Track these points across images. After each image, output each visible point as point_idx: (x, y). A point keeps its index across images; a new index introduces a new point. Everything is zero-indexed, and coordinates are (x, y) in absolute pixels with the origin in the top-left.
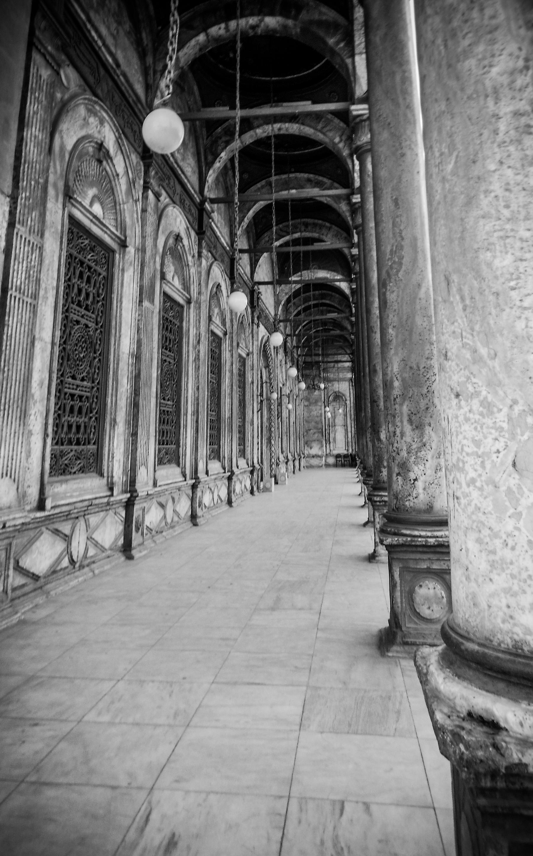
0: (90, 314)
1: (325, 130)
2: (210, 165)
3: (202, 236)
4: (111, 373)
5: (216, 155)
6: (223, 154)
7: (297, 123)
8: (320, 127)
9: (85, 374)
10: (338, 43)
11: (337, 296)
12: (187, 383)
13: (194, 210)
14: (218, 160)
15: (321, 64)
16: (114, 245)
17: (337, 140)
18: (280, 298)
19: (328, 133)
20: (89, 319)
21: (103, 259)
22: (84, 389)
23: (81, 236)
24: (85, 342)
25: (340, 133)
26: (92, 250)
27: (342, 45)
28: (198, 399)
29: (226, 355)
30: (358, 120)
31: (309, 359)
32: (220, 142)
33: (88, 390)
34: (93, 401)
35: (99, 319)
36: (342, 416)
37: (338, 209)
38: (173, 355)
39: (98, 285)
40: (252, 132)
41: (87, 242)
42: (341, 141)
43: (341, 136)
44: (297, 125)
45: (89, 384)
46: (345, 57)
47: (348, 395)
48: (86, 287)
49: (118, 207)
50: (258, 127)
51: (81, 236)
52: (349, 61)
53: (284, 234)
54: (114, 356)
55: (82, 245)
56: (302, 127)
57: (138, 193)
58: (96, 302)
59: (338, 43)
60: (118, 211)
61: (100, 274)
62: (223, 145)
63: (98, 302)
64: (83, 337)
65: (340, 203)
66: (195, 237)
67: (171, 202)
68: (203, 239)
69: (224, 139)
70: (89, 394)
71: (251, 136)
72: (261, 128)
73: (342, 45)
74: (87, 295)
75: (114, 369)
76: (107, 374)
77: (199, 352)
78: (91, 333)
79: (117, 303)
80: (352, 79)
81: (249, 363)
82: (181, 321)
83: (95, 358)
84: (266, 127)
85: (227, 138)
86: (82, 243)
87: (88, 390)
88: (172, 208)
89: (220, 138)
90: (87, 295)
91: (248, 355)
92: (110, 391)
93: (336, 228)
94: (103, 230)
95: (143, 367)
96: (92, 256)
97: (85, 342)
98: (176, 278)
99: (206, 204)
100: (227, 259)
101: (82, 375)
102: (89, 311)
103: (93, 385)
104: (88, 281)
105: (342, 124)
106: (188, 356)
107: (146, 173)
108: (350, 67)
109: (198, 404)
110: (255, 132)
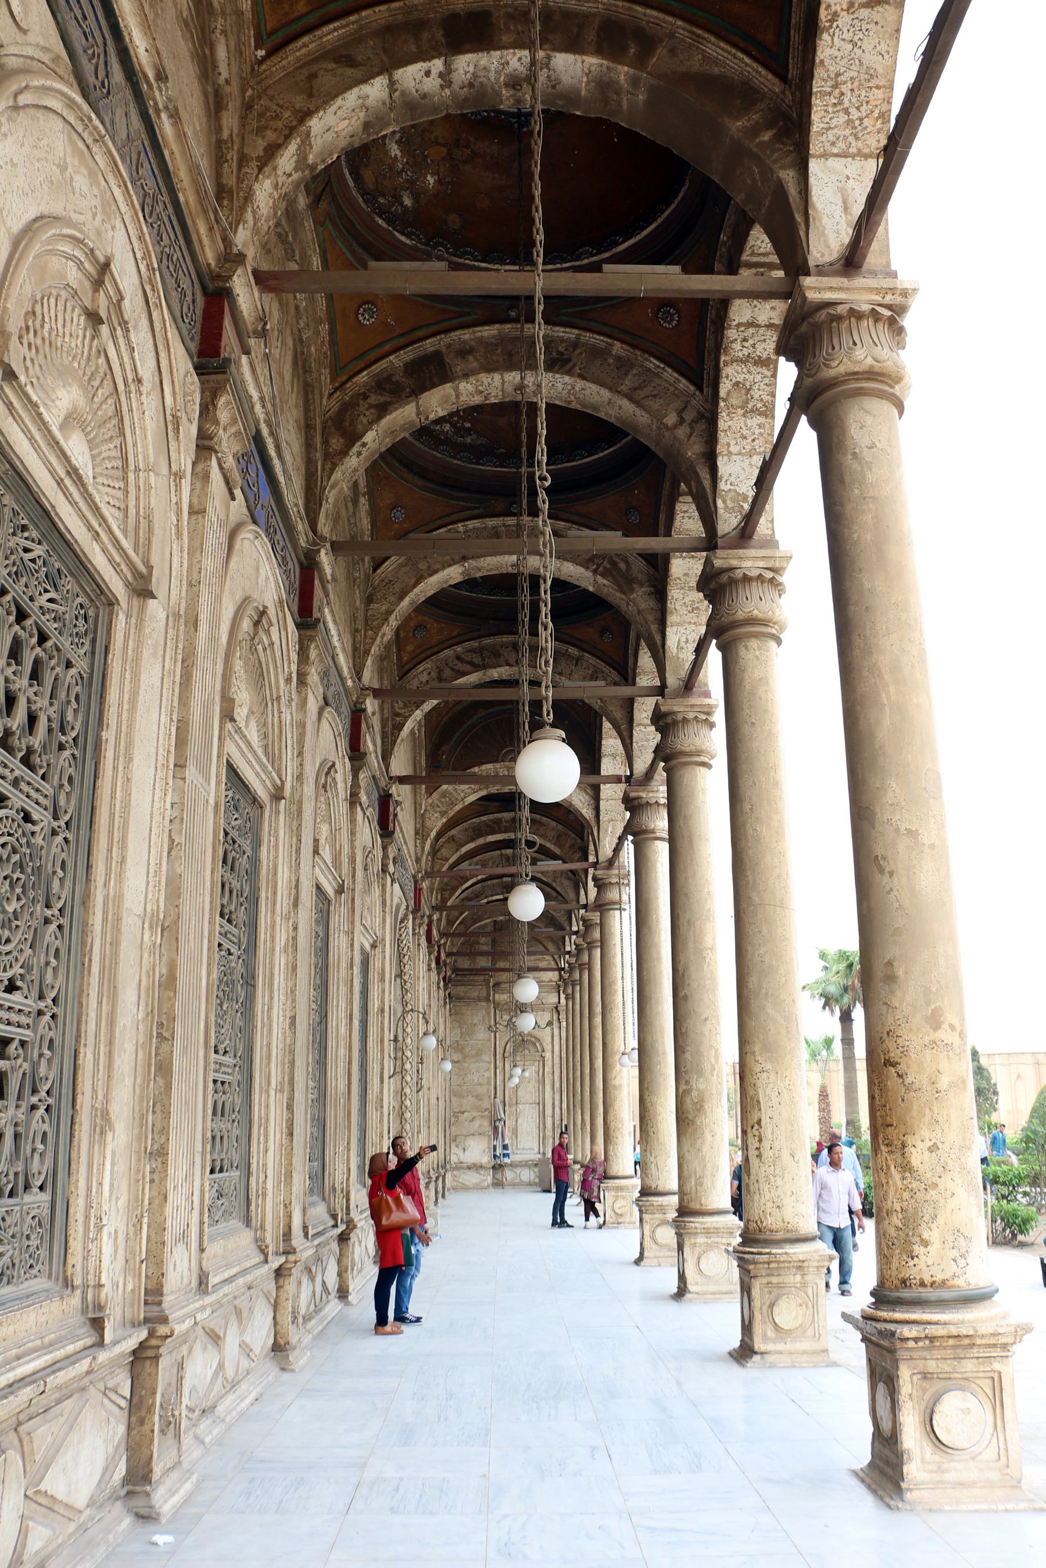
0: (35, 779)
1: (640, 394)
2: (333, 459)
3: (309, 633)
4: (95, 969)
5: (352, 437)
6: (369, 437)
7: (569, 373)
8: (628, 383)
9: (17, 970)
10: (754, 131)
11: (553, 824)
12: (270, 1009)
13: (294, 566)
14: (355, 449)
15: (676, 201)
16: (117, 587)
17: (671, 419)
18: (428, 823)
19: (646, 402)
20: (33, 793)
21: (81, 621)
22: (14, 1017)
23: (24, 528)
24: (21, 866)
25: (678, 404)
26: (53, 580)
27: (766, 136)
28: (292, 1052)
29: (339, 943)
30: (822, 315)
31: (464, 963)
32: (363, 405)
33: (24, 1020)
34: (41, 1055)
35: (62, 801)
36: (533, 1082)
37: (623, 606)
38: (235, 931)
39: (63, 696)
40: (448, 388)
41: (38, 551)
42: (682, 421)
43: (680, 413)
44: (567, 378)
45: (32, 1004)
46: (775, 167)
47: (549, 1039)
48: (31, 692)
49: (131, 476)
50: (466, 376)
51: (24, 528)
52: (788, 177)
53: (469, 668)
54: (105, 920)
55: (27, 556)
56: (580, 384)
57: (185, 458)
58: (55, 746)
59: (754, 131)
60: (132, 488)
61: (69, 665)
62: (371, 413)
63: (61, 747)
64: (14, 851)
65: (632, 591)
66: (293, 632)
67: (249, 520)
68: (311, 639)
69: (374, 399)
70: (27, 1034)
71: (445, 400)
72: (472, 379)
73: (766, 136)
74: (32, 719)
75: (103, 959)
76: (84, 969)
77: (295, 929)
78: (38, 840)
79: (116, 758)
80: (799, 218)
81: (376, 965)
82: (257, 844)
83: (47, 921)
84: (485, 378)
85: (386, 398)
86: (26, 550)
87: (24, 1020)
88: (251, 536)
89: (365, 397)
90: (32, 719)
91: (374, 946)
92: (92, 1026)
93: (593, 660)
94: (90, 527)
95: (181, 961)
96: (50, 601)
97: (21, 866)
98: (253, 724)
99: (323, 552)
100: (346, 710)
101: (10, 974)
102: (32, 768)
103: (42, 1005)
104: (35, 675)
105: (684, 384)
106: (273, 937)
107: (207, 409)
108: (792, 190)
109: (292, 1063)
110: (456, 389)
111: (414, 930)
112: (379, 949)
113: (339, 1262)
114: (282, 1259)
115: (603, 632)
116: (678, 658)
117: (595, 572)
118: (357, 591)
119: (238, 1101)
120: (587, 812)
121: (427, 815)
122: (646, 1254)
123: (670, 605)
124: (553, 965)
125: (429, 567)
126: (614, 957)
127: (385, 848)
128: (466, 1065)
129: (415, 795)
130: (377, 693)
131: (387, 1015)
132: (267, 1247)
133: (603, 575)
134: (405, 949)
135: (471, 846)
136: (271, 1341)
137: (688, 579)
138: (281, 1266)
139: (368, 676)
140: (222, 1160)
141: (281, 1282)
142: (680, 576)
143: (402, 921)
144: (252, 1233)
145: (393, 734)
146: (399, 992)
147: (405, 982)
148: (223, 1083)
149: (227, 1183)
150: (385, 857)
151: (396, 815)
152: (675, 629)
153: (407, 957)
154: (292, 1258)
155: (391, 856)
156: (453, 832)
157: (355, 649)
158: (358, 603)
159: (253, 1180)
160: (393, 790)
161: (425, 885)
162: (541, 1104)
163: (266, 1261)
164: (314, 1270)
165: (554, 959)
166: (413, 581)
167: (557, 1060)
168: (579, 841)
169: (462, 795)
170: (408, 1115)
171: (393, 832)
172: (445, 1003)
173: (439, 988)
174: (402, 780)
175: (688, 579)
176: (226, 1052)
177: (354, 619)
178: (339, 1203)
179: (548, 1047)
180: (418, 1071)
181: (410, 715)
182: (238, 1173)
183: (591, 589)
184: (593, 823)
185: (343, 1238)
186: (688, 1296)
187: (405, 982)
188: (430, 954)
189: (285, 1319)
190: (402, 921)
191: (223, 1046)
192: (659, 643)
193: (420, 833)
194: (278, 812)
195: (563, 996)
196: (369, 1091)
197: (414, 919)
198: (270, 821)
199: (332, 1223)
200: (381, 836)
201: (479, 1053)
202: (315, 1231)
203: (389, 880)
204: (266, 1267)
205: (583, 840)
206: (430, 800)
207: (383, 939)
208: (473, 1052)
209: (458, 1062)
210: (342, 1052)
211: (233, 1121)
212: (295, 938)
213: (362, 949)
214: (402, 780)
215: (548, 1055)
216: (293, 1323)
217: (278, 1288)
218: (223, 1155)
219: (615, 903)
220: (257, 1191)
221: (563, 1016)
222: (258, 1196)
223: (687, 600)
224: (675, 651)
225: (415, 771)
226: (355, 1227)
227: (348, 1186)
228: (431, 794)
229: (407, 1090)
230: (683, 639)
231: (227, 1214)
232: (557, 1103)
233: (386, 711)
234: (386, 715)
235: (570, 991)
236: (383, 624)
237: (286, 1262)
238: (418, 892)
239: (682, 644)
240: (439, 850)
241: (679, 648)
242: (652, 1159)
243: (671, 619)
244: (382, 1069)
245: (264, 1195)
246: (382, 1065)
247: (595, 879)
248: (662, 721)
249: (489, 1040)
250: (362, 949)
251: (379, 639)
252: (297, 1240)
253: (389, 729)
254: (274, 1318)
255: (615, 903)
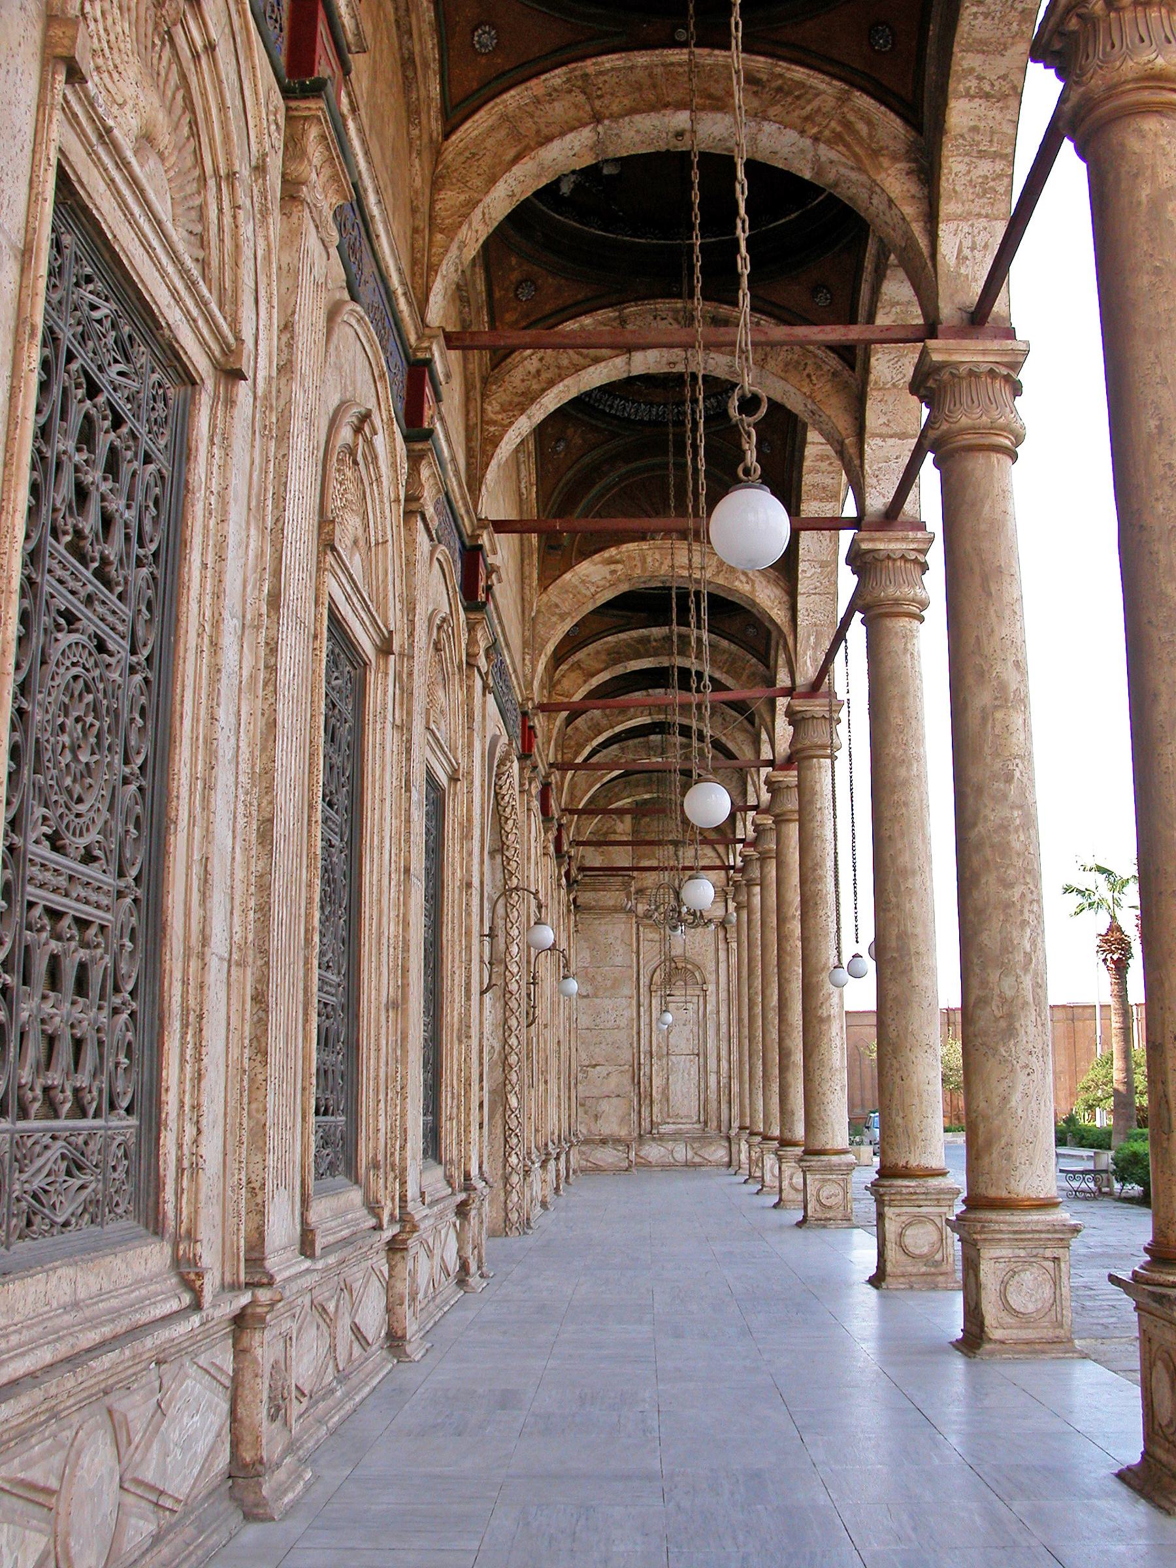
111: (521, 785)
112: (462, 786)
113: (388, 1288)
114: (245, 1299)
115: (815, 290)
116: (960, 274)
117: (816, 139)
118: (417, 162)
119: (130, 970)
120: (779, 615)
121: (541, 619)
122: (889, 1268)
123: (945, 185)
124: (718, 863)
125: (538, 132)
126: (822, 826)
127: (471, 628)
128: (597, 1001)
129: (523, 588)
130: (451, 341)
131: (475, 892)
132: (200, 1275)
133: (828, 142)
134: (508, 810)
135: (605, 676)
136: (223, 1460)
137: (978, 138)
138: (244, 1308)
139: (438, 310)
140: (77, 1091)
141: (245, 1342)
142: (965, 130)
143: (502, 763)
144: (168, 1249)
145: (483, 451)
146: (499, 876)
147: (509, 860)
148: (82, 924)
149: (94, 1146)
150: (472, 642)
151: (489, 589)
152: (953, 226)
153: (510, 822)
154: (264, 1295)
155: (483, 645)
156: (580, 655)
157: (414, 262)
158: (418, 183)
159: (168, 1140)
160: (485, 540)
161: (539, 722)
162: (700, 1054)
163: (197, 1306)
164: (331, 1307)
165: (719, 856)
166: (511, 154)
167: (723, 995)
168: (761, 668)
169: (593, 590)
170: (513, 1059)
171: (484, 604)
172: (569, 911)
173: (559, 885)
174: (500, 526)
175: (978, 138)
176: (88, 858)
177: (414, 211)
178: (385, 1191)
179: (711, 978)
180: (529, 995)
181: (512, 423)
182: (133, 1121)
183: (807, 176)
184: (786, 629)
185: (395, 1247)
186: (987, 1347)
187: (509, 860)
188: (546, 832)
189: (259, 1413)
190: (502, 763)
191: (83, 842)
192: (926, 251)
193: (531, 645)
194: (230, 403)
195: (732, 905)
196: (447, 1010)
197: (521, 769)
198: (213, 416)
199: (372, 1222)
200: (465, 609)
201: (616, 984)
202: (331, 1239)
203: (478, 683)
204: (196, 1320)
205: (768, 667)
206: (544, 597)
207: (470, 773)
208: (609, 983)
209: (587, 996)
210: (391, 929)
211: (116, 1011)
212: (272, 669)
213: (431, 779)
214: (500, 526)
215: (711, 988)
216: (273, 1418)
217: (240, 1352)
218: (83, 1080)
219: (824, 747)
220: (179, 1160)
221: (732, 934)
222: (180, 1170)
223: (974, 174)
224: (952, 262)
225: (521, 512)
226: (415, 1228)
227: (403, 1159)
228: (546, 588)
229: (513, 1022)
230: (967, 243)
231: (95, 1210)
232: (724, 1053)
233: (472, 414)
234: (472, 421)
235: (743, 898)
236: (461, 223)
237: (254, 1303)
238: (528, 734)
239: (966, 252)
240: (559, 681)
241: (961, 258)
242: (899, 1120)
243: (947, 208)
244: (469, 977)
245: (196, 1168)
246: (469, 970)
247: (790, 713)
248: (927, 384)
249: (631, 967)
250: (431, 779)
251: (454, 251)
252: (282, 1260)
253: (477, 445)
254: (233, 1412)
255: (824, 747)
